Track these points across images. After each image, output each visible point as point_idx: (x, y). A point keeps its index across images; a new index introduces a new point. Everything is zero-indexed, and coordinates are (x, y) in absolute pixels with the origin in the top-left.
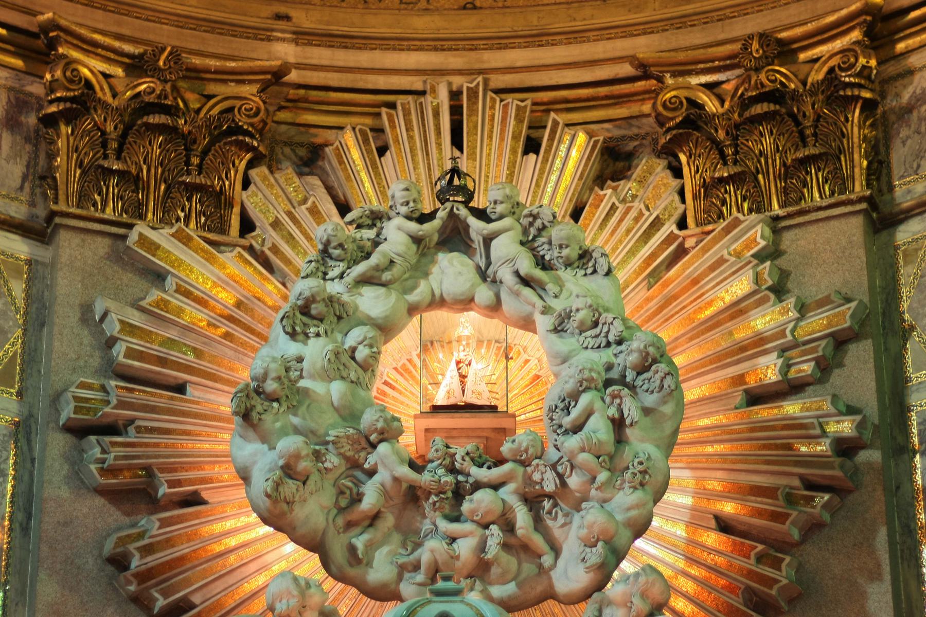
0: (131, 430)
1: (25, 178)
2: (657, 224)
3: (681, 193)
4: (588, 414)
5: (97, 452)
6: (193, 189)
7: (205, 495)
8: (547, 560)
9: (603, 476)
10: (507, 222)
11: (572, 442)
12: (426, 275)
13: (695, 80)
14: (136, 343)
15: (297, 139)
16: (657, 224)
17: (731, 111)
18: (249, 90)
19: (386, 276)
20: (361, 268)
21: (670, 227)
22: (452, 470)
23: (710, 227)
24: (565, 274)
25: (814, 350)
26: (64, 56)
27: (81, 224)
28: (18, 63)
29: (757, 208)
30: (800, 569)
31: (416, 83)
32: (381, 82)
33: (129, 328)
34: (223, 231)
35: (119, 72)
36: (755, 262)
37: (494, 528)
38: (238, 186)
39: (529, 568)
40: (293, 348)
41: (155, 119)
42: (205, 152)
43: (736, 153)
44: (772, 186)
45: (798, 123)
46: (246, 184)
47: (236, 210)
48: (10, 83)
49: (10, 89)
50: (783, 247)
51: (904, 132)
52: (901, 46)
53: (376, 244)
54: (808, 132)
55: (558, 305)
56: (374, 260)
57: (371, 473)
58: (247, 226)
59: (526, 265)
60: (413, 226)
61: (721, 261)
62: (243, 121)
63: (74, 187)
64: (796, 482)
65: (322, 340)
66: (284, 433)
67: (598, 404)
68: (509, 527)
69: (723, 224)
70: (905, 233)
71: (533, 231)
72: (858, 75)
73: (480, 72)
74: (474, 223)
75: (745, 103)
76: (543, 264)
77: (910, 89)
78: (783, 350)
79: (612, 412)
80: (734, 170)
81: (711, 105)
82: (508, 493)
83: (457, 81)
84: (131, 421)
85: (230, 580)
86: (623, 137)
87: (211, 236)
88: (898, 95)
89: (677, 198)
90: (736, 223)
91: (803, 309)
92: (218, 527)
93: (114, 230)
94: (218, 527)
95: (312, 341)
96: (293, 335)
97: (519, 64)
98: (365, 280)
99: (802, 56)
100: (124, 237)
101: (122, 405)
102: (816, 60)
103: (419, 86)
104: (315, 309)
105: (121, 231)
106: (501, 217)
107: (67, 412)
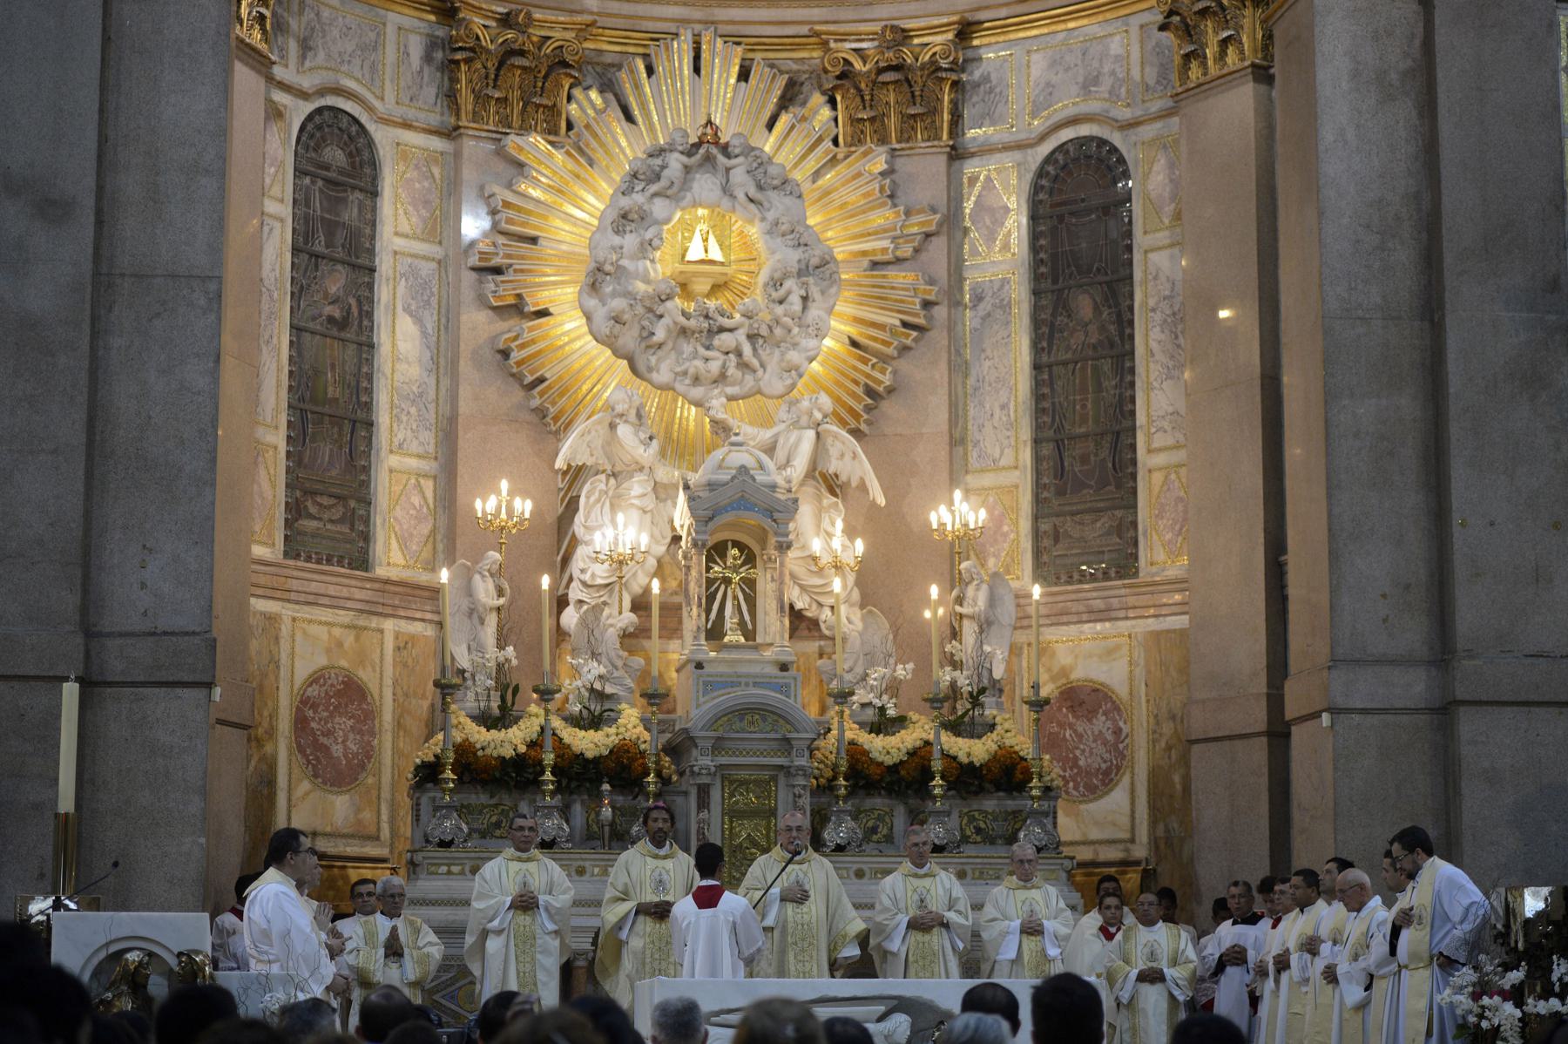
0: (511, 270)
1: (437, 97)
2: (820, 140)
3: (836, 120)
4: (789, 293)
5: (492, 286)
6: (538, 106)
7: (551, 310)
8: (760, 372)
9: (796, 330)
10: (740, 159)
11: (779, 310)
12: (690, 189)
13: (848, 45)
14: (511, 213)
15: (595, 60)
16: (820, 140)
17: (869, 72)
18: (570, 35)
19: (669, 192)
20: (654, 188)
21: (828, 144)
22: (707, 317)
23: (853, 149)
24: (772, 195)
25: (913, 241)
26: (464, 19)
27: (477, 133)
28: (432, 18)
29: (883, 140)
30: (895, 372)
31: (672, 28)
32: (650, 26)
33: (507, 204)
34: (556, 133)
35: (494, 24)
36: (880, 178)
37: (731, 356)
38: (565, 101)
39: (749, 378)
40: (617, 240)
41: (518, 61)
42: (546, 77)
43: (872, 100)
44: (893, 123)
45: (911, 86)
46: (569, 99)
47: (564, 116)
48: (426, 31)
49: (428, 35)
50: (896, 167)
51: (975, 99)
52: (976, 42)
53: (663, 167)
54: (917, 93)
55: (771, 215)
56: (663, 183)
57: (661, 316)
58: (570, 126)
59: (753, 192)
60: (684, 159)
61: (859, 175)
62: (569, 58)
63: (470, 107)
64: (898, 323)
65: (634, 235)
66: (614, 295)
67: (795, 288)
68: (739, 354)
69: (862, 149)
70: (970, 168)
71: (755, 165)
72: (952, 63)
73: (712, 23)
74: (721, 158)
75: (880, 71)
76: (760, 188)
77: (981, 70)
78: (894, 239)
79: (803, 293)
80: (872, 114)
81: (858, 65)
82: (741, 335)
83: (698, 27)
84: (511, 265)
85: (566, 362)
86: (799, 71)
87: (551, 138)
88: (972, 73)
89: (833, 124)
90: (871, 150)
91: (908, 213)
92: (559, 331)
93: (494, 136)
94: (559, 331)
95: (628, 236)
96: (617, 232)
97: (737, 19)
98: (655, 195)
99: (916, 41)
100: (500, 140)
101: (509, 256)
102: (927, 45)
103: (674, 30)
104: (630, 217)
105: (499, 136)
106: (736, 156)
107: (474, 260)
